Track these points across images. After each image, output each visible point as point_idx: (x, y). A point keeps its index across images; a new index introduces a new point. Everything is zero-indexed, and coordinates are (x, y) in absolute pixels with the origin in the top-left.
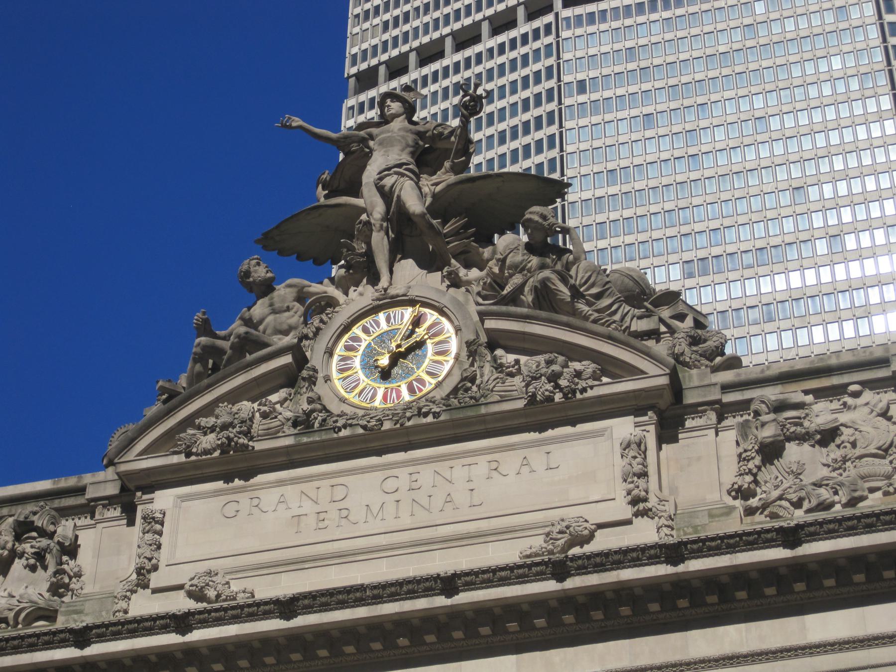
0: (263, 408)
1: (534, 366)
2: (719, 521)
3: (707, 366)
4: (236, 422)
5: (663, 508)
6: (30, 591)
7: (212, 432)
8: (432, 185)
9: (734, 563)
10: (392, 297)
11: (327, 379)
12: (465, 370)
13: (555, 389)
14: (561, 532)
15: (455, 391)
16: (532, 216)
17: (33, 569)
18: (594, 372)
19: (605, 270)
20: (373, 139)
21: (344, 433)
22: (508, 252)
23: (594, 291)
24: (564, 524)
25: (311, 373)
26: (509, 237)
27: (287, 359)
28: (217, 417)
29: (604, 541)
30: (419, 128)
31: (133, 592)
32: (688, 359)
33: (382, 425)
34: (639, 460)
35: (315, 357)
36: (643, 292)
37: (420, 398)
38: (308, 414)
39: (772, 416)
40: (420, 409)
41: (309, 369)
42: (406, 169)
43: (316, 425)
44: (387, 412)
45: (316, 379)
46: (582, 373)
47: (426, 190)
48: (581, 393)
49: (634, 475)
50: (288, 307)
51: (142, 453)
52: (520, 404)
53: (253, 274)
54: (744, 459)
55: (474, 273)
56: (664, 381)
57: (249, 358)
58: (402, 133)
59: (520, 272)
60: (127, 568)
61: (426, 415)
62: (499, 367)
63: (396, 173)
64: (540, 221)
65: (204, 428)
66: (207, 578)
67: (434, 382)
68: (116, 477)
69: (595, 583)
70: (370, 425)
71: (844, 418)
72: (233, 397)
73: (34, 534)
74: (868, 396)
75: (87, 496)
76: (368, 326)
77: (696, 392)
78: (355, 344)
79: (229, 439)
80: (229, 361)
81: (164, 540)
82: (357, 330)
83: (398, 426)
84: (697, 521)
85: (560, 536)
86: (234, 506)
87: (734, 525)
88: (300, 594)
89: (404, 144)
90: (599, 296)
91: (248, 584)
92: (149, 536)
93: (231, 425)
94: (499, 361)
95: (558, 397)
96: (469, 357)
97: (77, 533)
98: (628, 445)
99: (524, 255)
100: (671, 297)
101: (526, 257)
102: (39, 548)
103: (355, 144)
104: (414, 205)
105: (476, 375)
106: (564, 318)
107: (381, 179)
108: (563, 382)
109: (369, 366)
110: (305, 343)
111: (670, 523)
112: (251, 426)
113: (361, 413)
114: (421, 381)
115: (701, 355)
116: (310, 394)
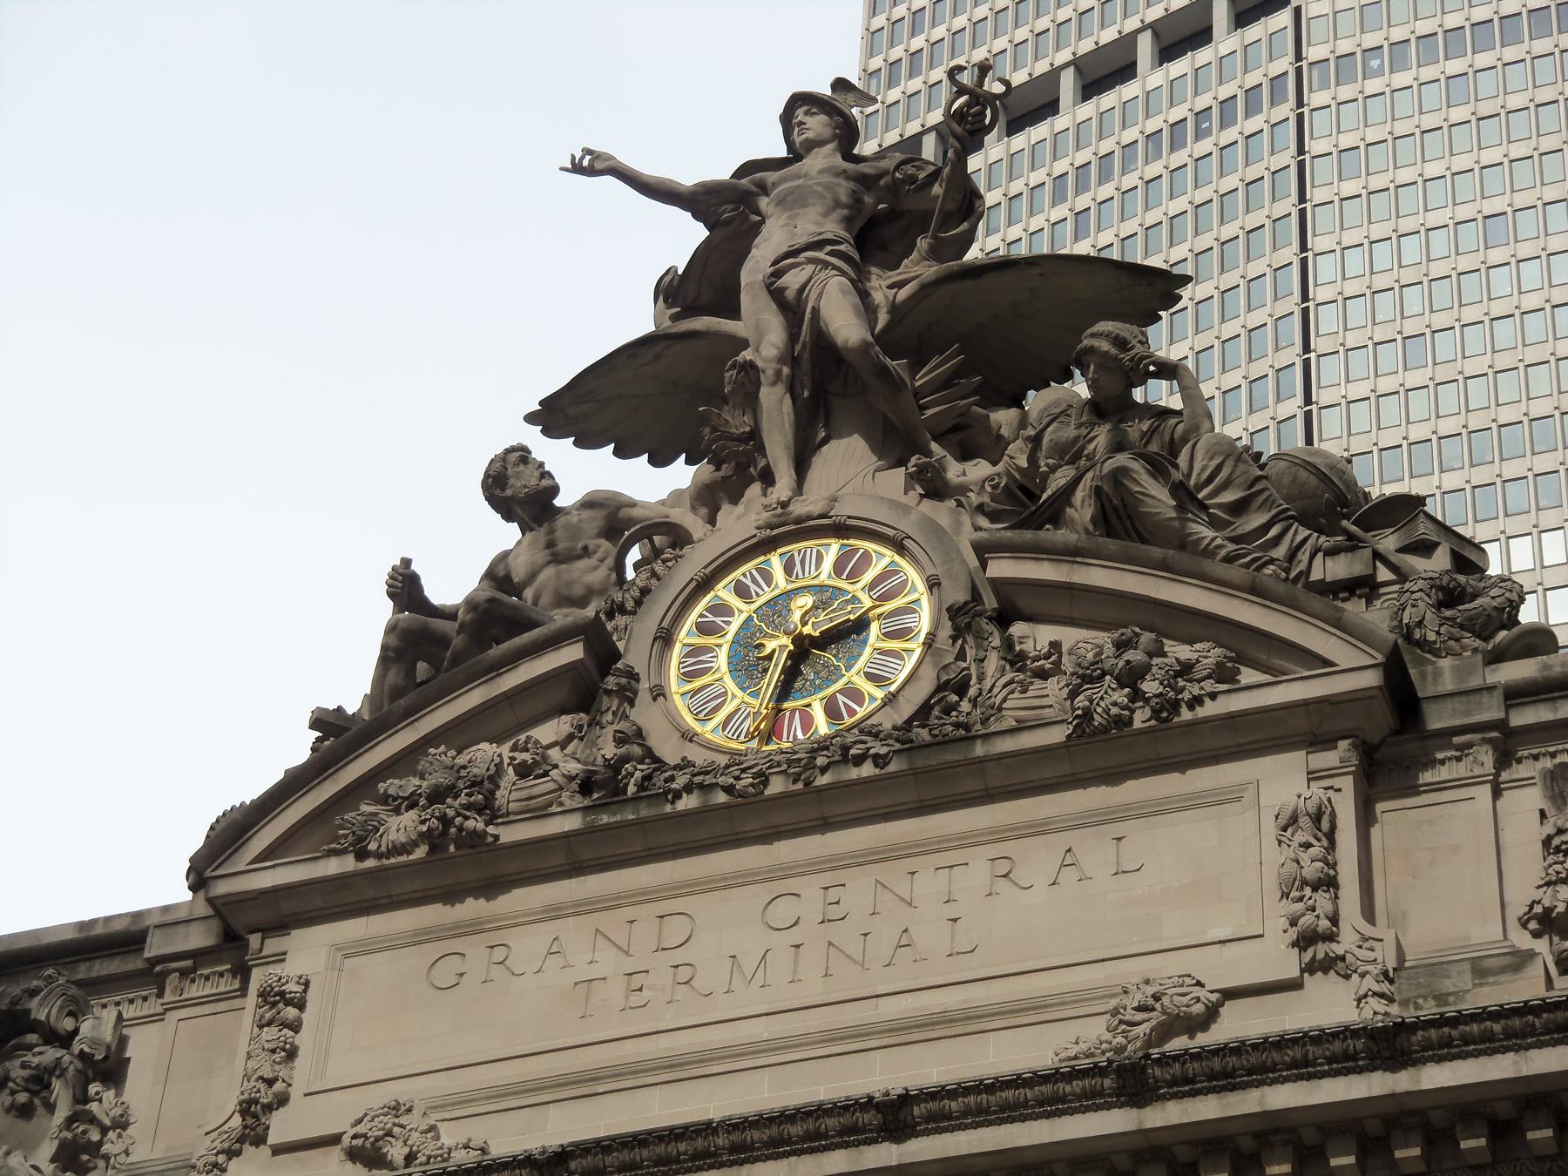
0: (522, 756)
1: (1090, 656)
2: (1494, 983)
3: (1475, 650)
4: (461, 784)
5: (1370, 955)
7: (411, 807)
8: (890, 287)
9: (1524, 1072)
10: (798, 521)
11: (659, 693)
12: (945, 667)
13: (1133, 701)
14: (1140, 1009)
15: (924, 711)
16: (1096, 343)
18: (1219, 665)
19: (1260, 454)
20: (766, 192)
21: (688, 802)
22: (1045, 422)
23: (1229, 497)
24: (1150, 990)
25: (624, 681)
26: (1055, 392)
27: (573, 652)
28: (422, 778)
29: (1240, 1024)
30: (863, 168)
31: (232, 1154)
32: (1431, 637)
33: (766, 783)
34: (1316, 851)
35: (635, 652)
36: (1345, 504)
37: (849, 729)
38: (615, 766)
40: (845, 749)
41: (621, 673)
42: (830, 253)
43: (631, 789)
44: (777, 758)
45: (636, 693)
46: (1192, 666)
47: (879, 297)
48: (1191, 707)
49: (1305, 883)
50: (585, 548)
51: (261, 857)
52: (1057, 735)
53: (511, 481)
54: (1558, 850)
55: (979, 470)
56: (1370, 679)
57: (496, 651)
58: (826, 179)
59: (1072, 462)
60: (223, 1107)
61: (858, 761)
62: (1015, 658)
63: (811, 261)
64: (1113, 351)
65: (395, 799)
66: (389, 1120)
67: (880, 694)
68: (211, 912)
69: (1211, 1116)
70: (740, 785)
72: (459, 733)
73: (32, 1038)
75: (147, 954)
76: (748, 582)
77: (1448, 705)
78: (718, 620)
79: (445, 821)
80: (457, 660)
81: (303, 1040)
82: (723, 591)
83: (800, 786)
84: (1448, 982)
85: (1140, 1016)
86: (453, 964)
87: (1527, 987)
88: (577, 1145)
89: (830, 202)
90: (1239, 508)
91: (477, 1130)
92: (270, 1033)
93: (450, 791)
94: (1018, 648)
95: (1141, 718)
96: (954, 639)
97: (125, 1031)
98: (1294, 820)
99: (1079, 426)
100: (1406, 508)
101: (1084, 431)
102: (37, 1067)
103: (730, 207)
104: (845, 324)
105: (969, 677)
106: (1157, 552)
107: (778, 274)
108: (1150, 687)
109: (748, 665)
110: (621, 620)
111: (1385, 987)
112: (492, 793)
113: (723, 760)
114: (855, 694)
115: (1462, 627)
116: (623, 726)
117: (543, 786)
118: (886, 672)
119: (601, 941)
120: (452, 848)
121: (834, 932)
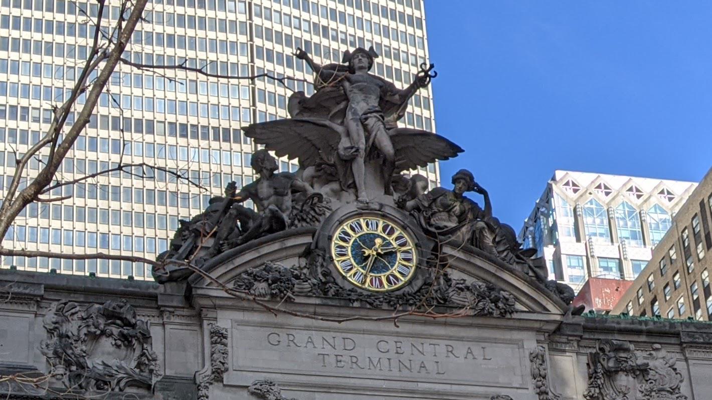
6: (124, 364)
15: (419, 291)
17: (118, 347)
31: (211, 384)
39: (612, 354)
48: (510, 314)
49: (540, 375)
61: (411, 305)
71: (651, 364)
73: (119, 322)
74: (663, 353)
95: (496, 313)
117: (307, 286)
118: (402, 271)
119: (325, 342)
120: (279, 299)
121: (402, 358)
